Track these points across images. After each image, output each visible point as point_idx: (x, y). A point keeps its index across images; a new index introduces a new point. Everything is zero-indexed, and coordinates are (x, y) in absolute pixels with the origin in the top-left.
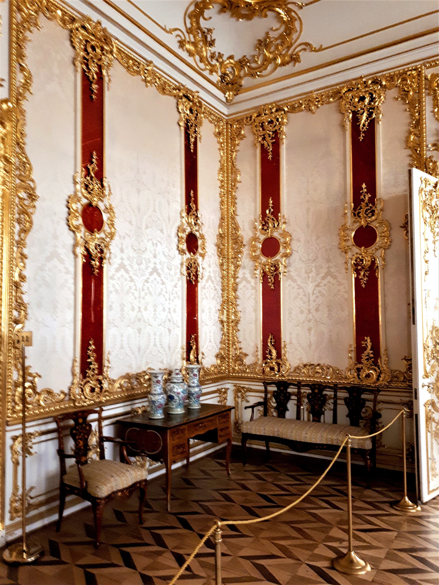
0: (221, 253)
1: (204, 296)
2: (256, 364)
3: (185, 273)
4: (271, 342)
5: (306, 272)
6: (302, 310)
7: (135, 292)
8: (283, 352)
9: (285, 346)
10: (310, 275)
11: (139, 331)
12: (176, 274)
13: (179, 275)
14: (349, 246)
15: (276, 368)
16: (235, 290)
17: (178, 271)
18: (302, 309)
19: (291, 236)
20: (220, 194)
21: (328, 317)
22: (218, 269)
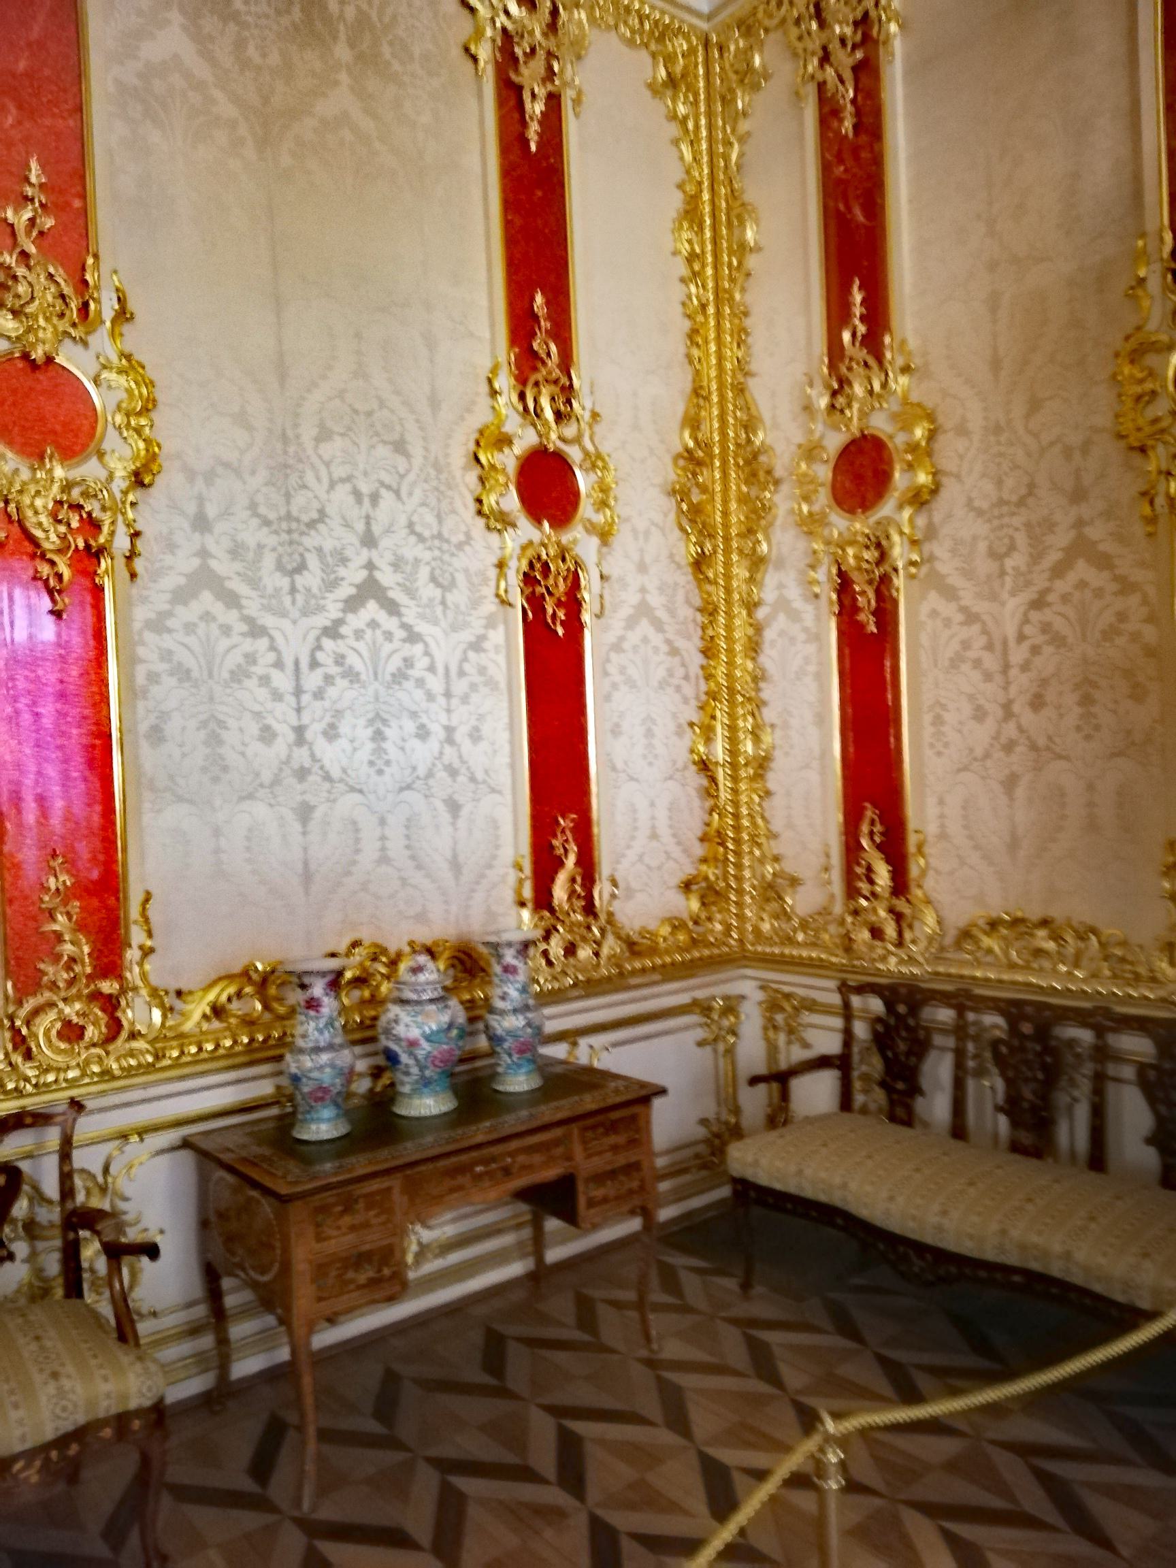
0: (694, 517)
1: (618, 678)
2: (825, 911)
3: (518, 600)
4: (871, 834)
5: (993, 554)
6: (979, 708)
7: (683, 683)
8: (914, 871)
9: (920, 848)
10: (1009, 563)
11: (305, 812)
12: (475, 603)
13: (490, 606)
14: (1156, 421)
15: (890, 931)
16: (754, 648)
17: (489, 591)
18: (982, 701)
19: (931, 417)
20: (684, 304)
21: (1078, 728)
22: (685, 578)
